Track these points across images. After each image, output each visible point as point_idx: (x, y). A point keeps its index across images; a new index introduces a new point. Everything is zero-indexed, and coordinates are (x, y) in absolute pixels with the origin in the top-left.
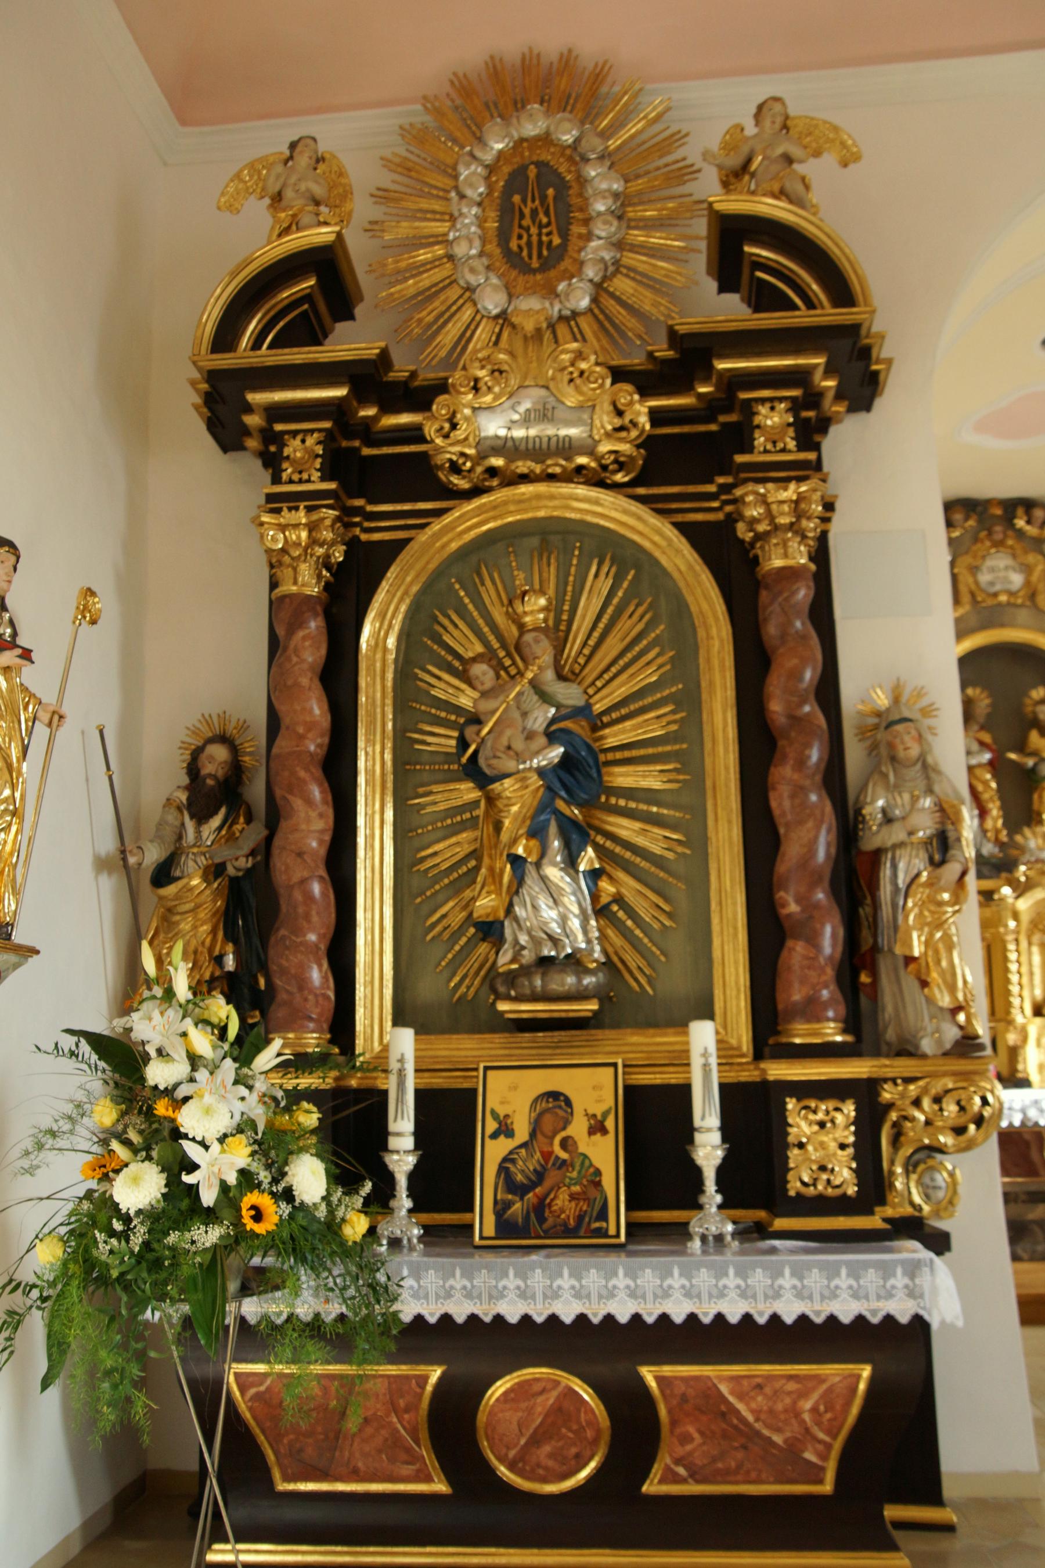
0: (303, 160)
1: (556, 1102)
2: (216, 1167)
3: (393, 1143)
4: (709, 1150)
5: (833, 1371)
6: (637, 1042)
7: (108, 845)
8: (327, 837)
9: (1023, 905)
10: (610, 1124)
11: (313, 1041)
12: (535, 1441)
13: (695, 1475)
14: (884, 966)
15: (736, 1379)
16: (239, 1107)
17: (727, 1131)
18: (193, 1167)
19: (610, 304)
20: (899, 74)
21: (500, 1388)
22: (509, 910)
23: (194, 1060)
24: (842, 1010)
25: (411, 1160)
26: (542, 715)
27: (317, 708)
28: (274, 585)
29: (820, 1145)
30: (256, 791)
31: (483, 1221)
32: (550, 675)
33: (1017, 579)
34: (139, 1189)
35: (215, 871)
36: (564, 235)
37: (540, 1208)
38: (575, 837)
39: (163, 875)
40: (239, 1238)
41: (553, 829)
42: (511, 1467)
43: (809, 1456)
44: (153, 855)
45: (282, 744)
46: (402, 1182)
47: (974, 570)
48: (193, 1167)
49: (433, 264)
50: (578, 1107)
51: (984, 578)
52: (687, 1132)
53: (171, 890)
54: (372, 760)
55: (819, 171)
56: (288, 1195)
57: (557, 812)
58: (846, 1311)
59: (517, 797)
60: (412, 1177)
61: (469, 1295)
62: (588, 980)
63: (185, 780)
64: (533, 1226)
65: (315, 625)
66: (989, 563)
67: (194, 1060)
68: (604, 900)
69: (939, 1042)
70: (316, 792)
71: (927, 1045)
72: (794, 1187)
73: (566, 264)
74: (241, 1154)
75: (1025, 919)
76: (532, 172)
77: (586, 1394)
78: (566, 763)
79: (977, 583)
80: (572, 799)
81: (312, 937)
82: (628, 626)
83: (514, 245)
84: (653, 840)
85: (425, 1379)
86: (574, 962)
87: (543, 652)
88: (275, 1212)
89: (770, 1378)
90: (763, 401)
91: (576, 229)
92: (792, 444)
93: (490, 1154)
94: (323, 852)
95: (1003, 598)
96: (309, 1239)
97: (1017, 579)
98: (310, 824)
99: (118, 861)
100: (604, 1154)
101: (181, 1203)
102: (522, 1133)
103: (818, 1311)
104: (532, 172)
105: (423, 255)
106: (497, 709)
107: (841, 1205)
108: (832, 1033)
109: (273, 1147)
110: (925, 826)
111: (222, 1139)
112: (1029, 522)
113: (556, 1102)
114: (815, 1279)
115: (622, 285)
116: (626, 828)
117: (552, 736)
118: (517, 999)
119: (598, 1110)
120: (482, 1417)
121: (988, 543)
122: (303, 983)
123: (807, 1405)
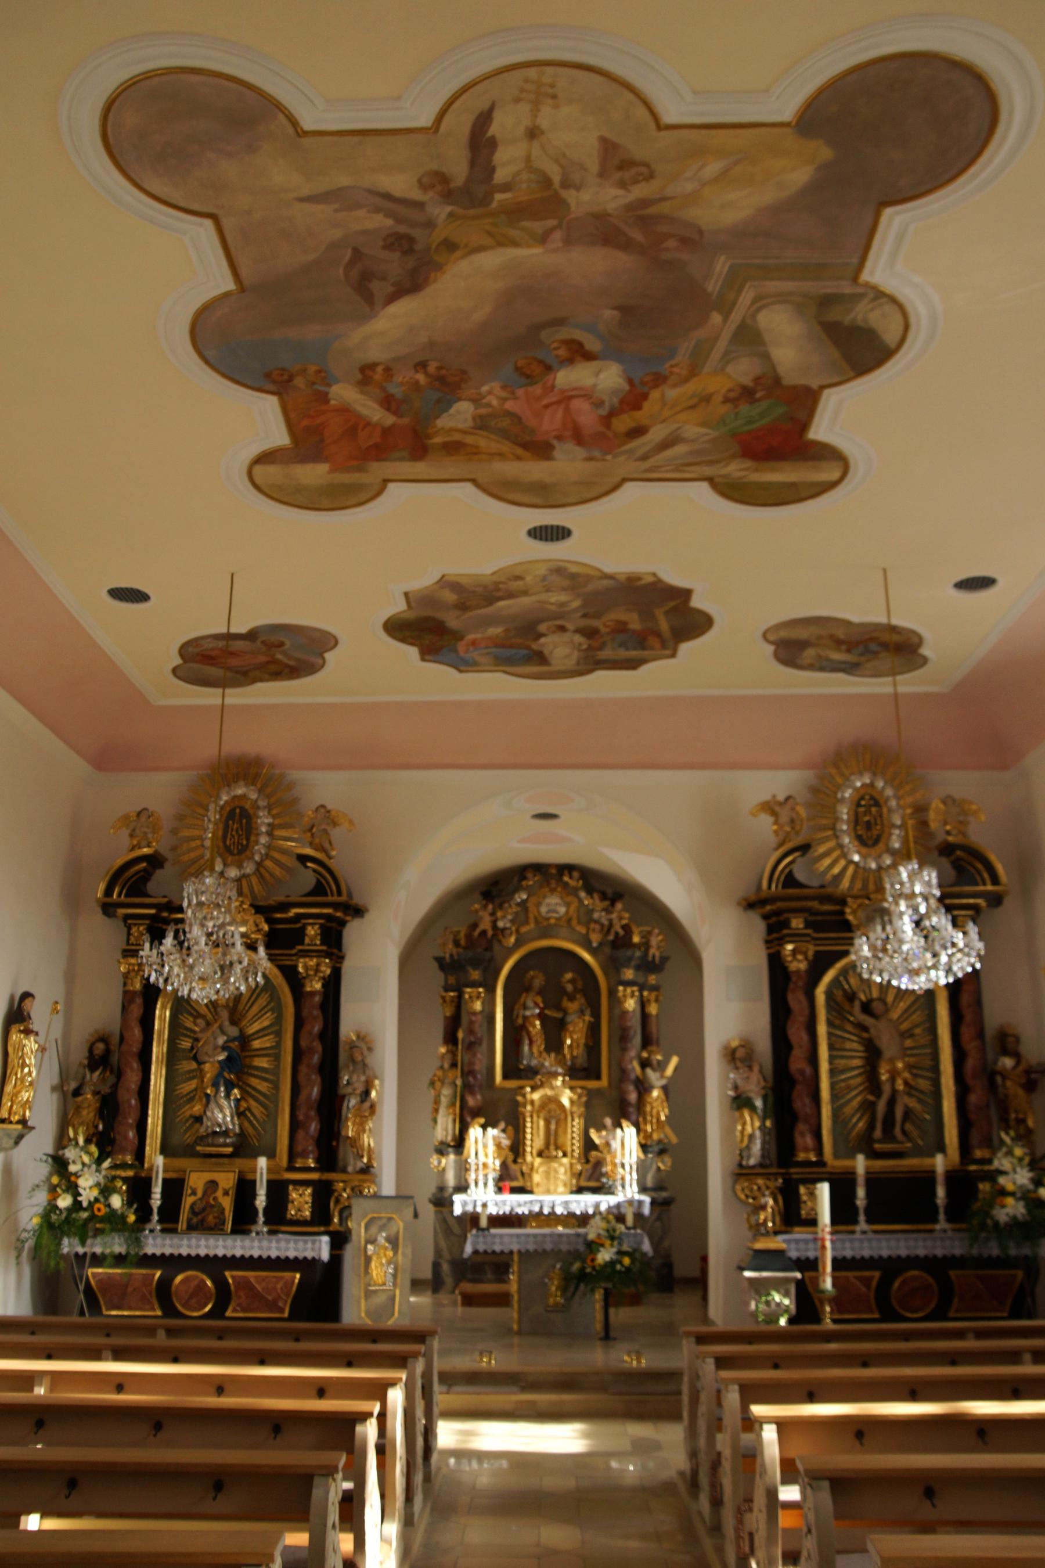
0: (143, 819)
1: (213, 1184)
3: (154, 1196)
4: (261, 1201)
5: (287, 1275)
6: (240, 1163)
7: (56, 1080)
8: (139, 1083)
9: (536, 1096)
10: (230, 1192)
11: (129, 1159)
12: (191, 1297)
13: (243, 1310)
14: (341, 1140)
15: (256, 1277)
16: (96, 1179)
17: (269, 1195)
18: (80, 1195)
19: (262, 871)
20: (388, 775)
21: (179, 1278)
22: (205, 1112)
23: (84, 1164)
24: (316, 1154)
25: (159, 1203)
26: (221, 1040)
27: (137, 1033)
28: (125, 984)
30: (114, 1059)
31: (182, 1225)
32: (227, 1023)
33: (562, 910)
34: (64, 1202)
35: (96, 1093)
36: (248, 839)
37: (202, 1221)
38: (229, 1087)
39: (77, 1093)
40: (93, 1217)
41: (222, 1082)
42: (183, 1306)
43: (281, 1304)
44: (73, 1085)
45: (124, 1048)
46: (155, 1210)
47: (538, 905)
48: (80, 1195)
49: (197, 848)
50: (220, 1186)
51: (543, 910)
52: (254, 1195)
53: (79, 1099)
54: (158, 1050)
55: (335, 833)
56: (109, 1206)
57: (225, 1078)
58: (291, 1254)
59: (210, 1070)
60: (160, 1209)
61: (171, 1246)
62: (228, 1141)
63: (87, 1054)
65: (139, 1001)
66: (547, 901)
67: (84, 1164)
68: (242, 1109)
69: (354, 1168)
70: (135, 1065)
71: (350, 1169)
72: (289, 1216)
73: (248, 853)
74: (95, 1193)
75: (537, 1104)
76: (238, 811)
77: (209, 1283)
78: (229, 1059)
79: (539, 912)
80: (231, 1072)
81: (130, 1121)
83: (228, 842)
84: (263, 1087)
85: (154, 1275)
86: (226, 1133)
88: (104, 1210)
89: (267, 1277)
90: (309, 924)
91: (253, 838)
92: (318, 942)
93: (188, 1201)
94: (137, 1089)
95: (552, 921)
96: (114, 1221)
97: (562, 910)
98: (132, 1079)
99: (59, 1088)
100: (227, 1203)
101: (77, 1205)
102: (200, 1194)
103: (283, 1255)
104: (238, 811)
105: (193, 844)
106: (203, 1037)
107: (304, 1223)
109: (106, 1191)
110: (360, 1088)
111: (91, 1188)
112: (571, 877)
113: (213, 1184)
114: (283, 1244)
115: (268, 863)
116: (254, 1082)
117: (224, 1048)
118: (205, 1146)
119: (227, 1187)
120: (173, 1288)
121: (547, 889)
122: (126, 1137)
123: (279, 1286)
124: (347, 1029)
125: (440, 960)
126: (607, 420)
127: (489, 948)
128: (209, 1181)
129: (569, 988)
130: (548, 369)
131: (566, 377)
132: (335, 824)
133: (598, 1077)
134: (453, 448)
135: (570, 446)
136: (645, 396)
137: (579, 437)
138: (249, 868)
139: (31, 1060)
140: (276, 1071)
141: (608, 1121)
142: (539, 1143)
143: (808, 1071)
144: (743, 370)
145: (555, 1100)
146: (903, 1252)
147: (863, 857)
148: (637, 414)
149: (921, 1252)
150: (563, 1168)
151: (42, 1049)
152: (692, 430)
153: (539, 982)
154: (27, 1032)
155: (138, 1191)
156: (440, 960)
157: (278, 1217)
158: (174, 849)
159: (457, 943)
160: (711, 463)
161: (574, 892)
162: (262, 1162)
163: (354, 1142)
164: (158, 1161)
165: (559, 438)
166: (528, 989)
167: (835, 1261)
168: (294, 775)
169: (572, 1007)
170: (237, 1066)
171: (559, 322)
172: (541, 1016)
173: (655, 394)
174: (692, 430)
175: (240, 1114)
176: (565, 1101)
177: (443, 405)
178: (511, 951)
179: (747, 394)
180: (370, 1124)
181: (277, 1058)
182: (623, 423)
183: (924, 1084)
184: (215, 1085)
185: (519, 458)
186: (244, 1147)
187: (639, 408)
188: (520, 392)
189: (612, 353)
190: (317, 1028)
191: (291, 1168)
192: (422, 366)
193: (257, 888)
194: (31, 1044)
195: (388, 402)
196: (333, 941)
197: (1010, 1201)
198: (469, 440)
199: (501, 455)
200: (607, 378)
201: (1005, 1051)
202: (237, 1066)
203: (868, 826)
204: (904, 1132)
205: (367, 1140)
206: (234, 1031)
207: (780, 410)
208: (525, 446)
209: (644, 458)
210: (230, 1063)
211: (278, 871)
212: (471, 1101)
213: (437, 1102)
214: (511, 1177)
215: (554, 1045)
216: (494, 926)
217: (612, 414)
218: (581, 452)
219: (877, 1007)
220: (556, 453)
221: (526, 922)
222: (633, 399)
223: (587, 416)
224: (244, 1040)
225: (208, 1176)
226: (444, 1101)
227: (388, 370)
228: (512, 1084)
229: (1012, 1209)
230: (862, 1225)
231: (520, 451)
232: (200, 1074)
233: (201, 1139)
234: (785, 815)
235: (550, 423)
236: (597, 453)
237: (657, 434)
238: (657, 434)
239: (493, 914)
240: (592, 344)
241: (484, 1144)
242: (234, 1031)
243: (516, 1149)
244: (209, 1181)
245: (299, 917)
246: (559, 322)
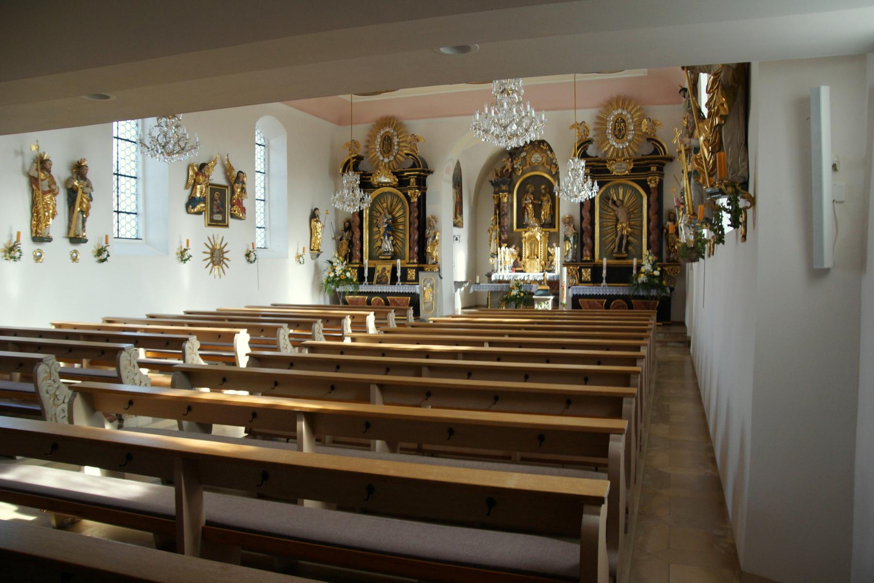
1: (384, 269)
2: (338, 273)
4: (399, 274)
9: (527, 235)
11: (358, 261)
27: (358, 219)
29: (411, 274)
31: (375, 282)
33: (540, 159)
34: (332, 275)
38: (389, 236)
39: (341, 239)
40: (340, 280)
44: (339, 237)
51: (533, 160)
54: (366, 224)
55: (418, 144)
59: (382, 230)
64: (385, 283)
82: (399, 206)
84: (401, 235)
86: (388, 252)
87: (386, 211)
93: (376, 274)
96: (349, 281)
97: (540, 159)
98: (357, 235)
100: (389, 275)
101: (335, 276)
108: (415, 261)
109: (345, 271)
110: (432, 235)
113: (384, 269)
115: (398, 156)
124: (429, 214)
125: (491, 182)
127: (511, 176)
128: (383, 268)
129: (543, 191)
132: (418, 141)
133: (554, 227)
138: (392, 158)
139: (319, 230)
140: (404, 230)
141: (554, 245)
142: (528, 253)
143: (589, 227)
145: (534, 237)
146: (615, 293)
147: (617, 143)
149: (621, 293)
150: (537, 263)
151: (324, 226)
153: (531, 190)
154: (317, 221)
155: (361, 270)
156: (491, 182)
157: (404, 279)
158: (366, 153)
159: (497, 175)
161: (545, 151)
162: (399, 261)
163: (431, 254)
164: (366, 261)
166: (527, 192)
168: (406, 122)
169: (545, 199)
170: (392, 229)
172: (532, 203)
175: (394, 245)
176: (538, 238)
178: (520, 177)
180: (436, 248)
181: (405, 225)
183: (637, 232)
184: (384, 235)
186: (394, 256)
190: (416, 215)
191: (409, 263)
193: (395, 165)
194: (319, 225)
196: (422, 183)
197: (642, 275)
201: (670, 220)
202: (392, 229)
203: (620, 130)
204: (627, 249)
205: (435, 254)
206: (390, 217)
210: (388, 228)
211: (402, 159)
212: (503, 238)
213: (491, 238)
214: (517, 266)
215: (537, 215)
216: (513, 168)
219: (618, 203)
221: (526, 165)
224: (394, 220)
225: (382, 266)
226: (493, 237)
228: (520, 230)
229: (642, 278)
230: (604, 283)
232: (379, 232)
233: (381, 254)
234: (582, 128)
239: (512, 161)
241: (507, 254)
242: (390, 217)
243: (520, 255)
244: (383, 268)
245: (408, 176)
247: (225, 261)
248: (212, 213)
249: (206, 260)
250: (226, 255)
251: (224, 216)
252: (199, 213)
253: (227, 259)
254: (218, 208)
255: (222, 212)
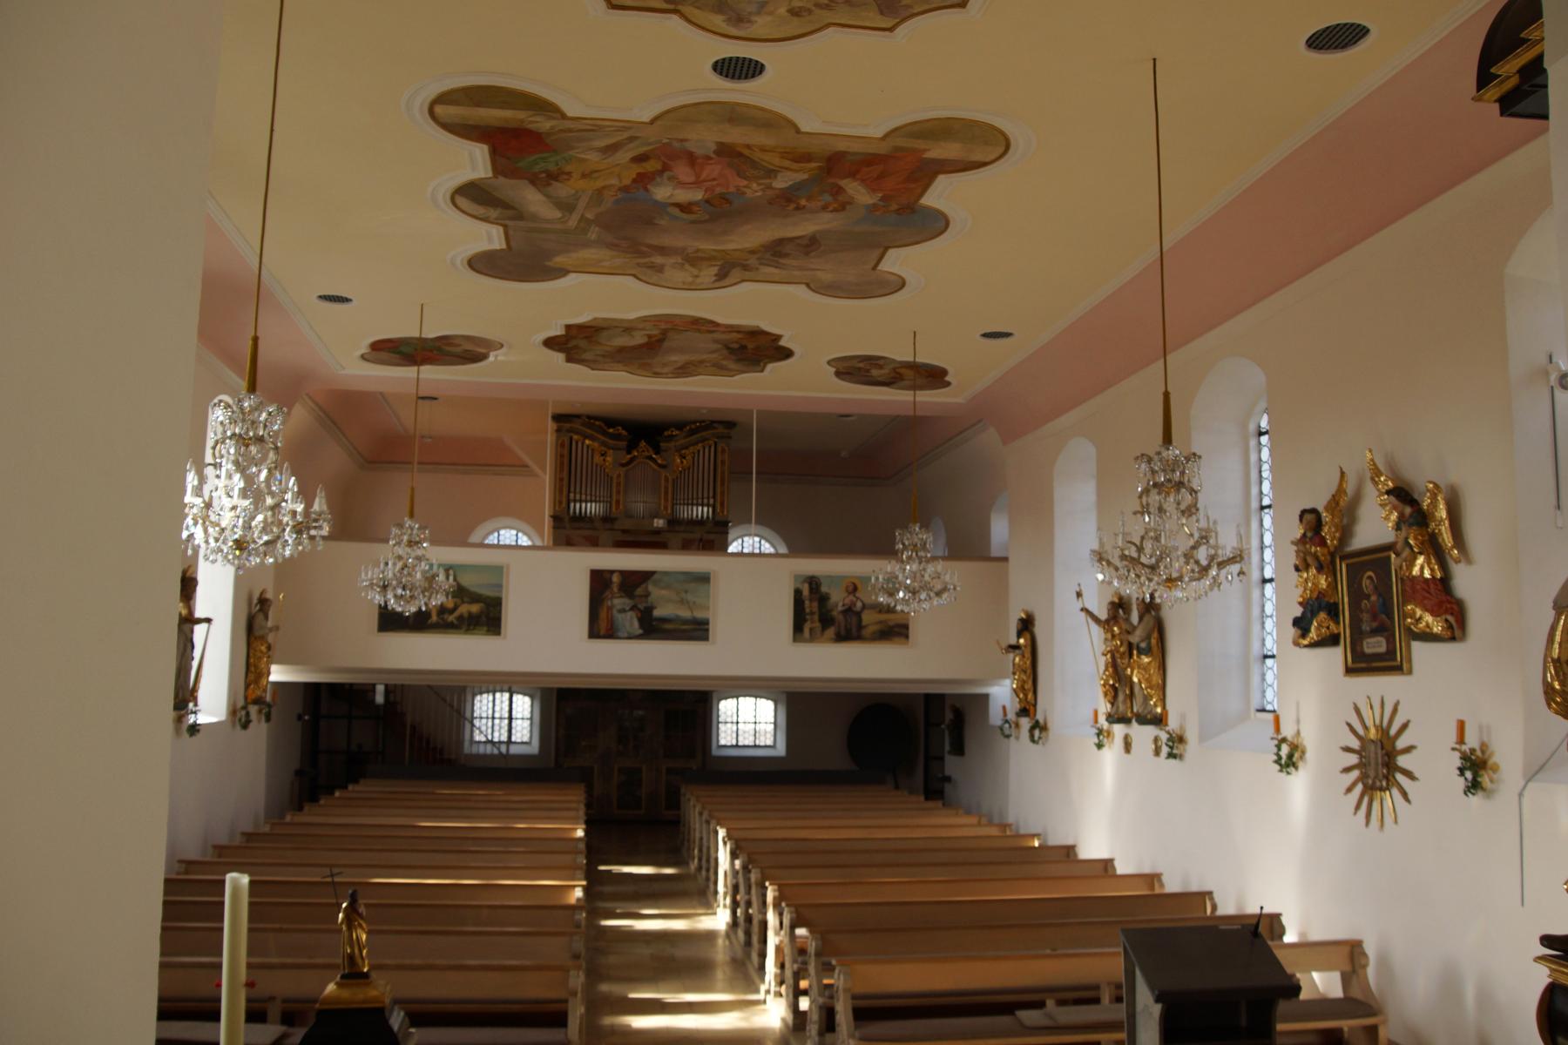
126: (666, 168)
130: (707, 201)
131: (698, 195)
134: (806, 158)
135: (699, 152)
136: (634, 181)
137: (692, 159)
144: (562, 190)
148: (641, 170)
152: (593, 157)
160: (570, 131)
165: (709, 158)
167: (218, 1019)
171: (693, 222)
173: (627, 181)
174: (593, 157)
177: (798, 187)
179: (553, 177)
182: (652, 166)
185: (748, 147)
187: (639, 174)
188: (732, 189)
189: (662, 207)
192: (798, 208)
195: (839, 190)
198: (787, 163)
199: (763, 149)
200: (662, 192)
207: (520, 164)
208: (740, 155)
209: (632, 139)
217: (661, 172)
218: (690, 146)
220: (714, 147)
222: (643, 180)
223: (683, 171)
227: (825, 208)
231: (746, 152)
235: (713, 170)
236: (676, 145)
237: (624, 156)
238: (624, 156)
240: (676, 212)
246: (693, 222)
247: (1400, 777)
248: (1357, 636)
249: (1347, 770)
250: (1353, 759)
251: (1391, 640)
252: (1331, 640)
253: (1409, 774)
254: (1374, 617)
255: (1384, 630)
